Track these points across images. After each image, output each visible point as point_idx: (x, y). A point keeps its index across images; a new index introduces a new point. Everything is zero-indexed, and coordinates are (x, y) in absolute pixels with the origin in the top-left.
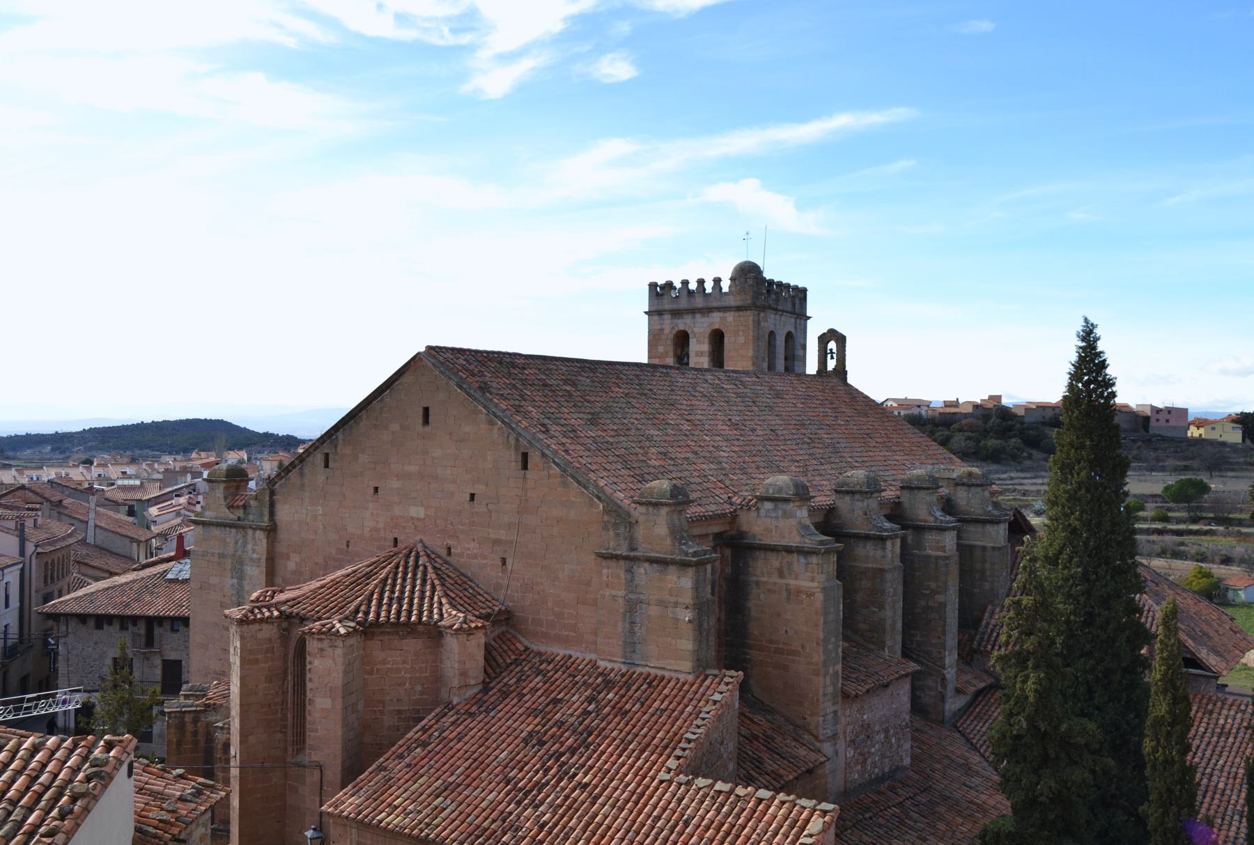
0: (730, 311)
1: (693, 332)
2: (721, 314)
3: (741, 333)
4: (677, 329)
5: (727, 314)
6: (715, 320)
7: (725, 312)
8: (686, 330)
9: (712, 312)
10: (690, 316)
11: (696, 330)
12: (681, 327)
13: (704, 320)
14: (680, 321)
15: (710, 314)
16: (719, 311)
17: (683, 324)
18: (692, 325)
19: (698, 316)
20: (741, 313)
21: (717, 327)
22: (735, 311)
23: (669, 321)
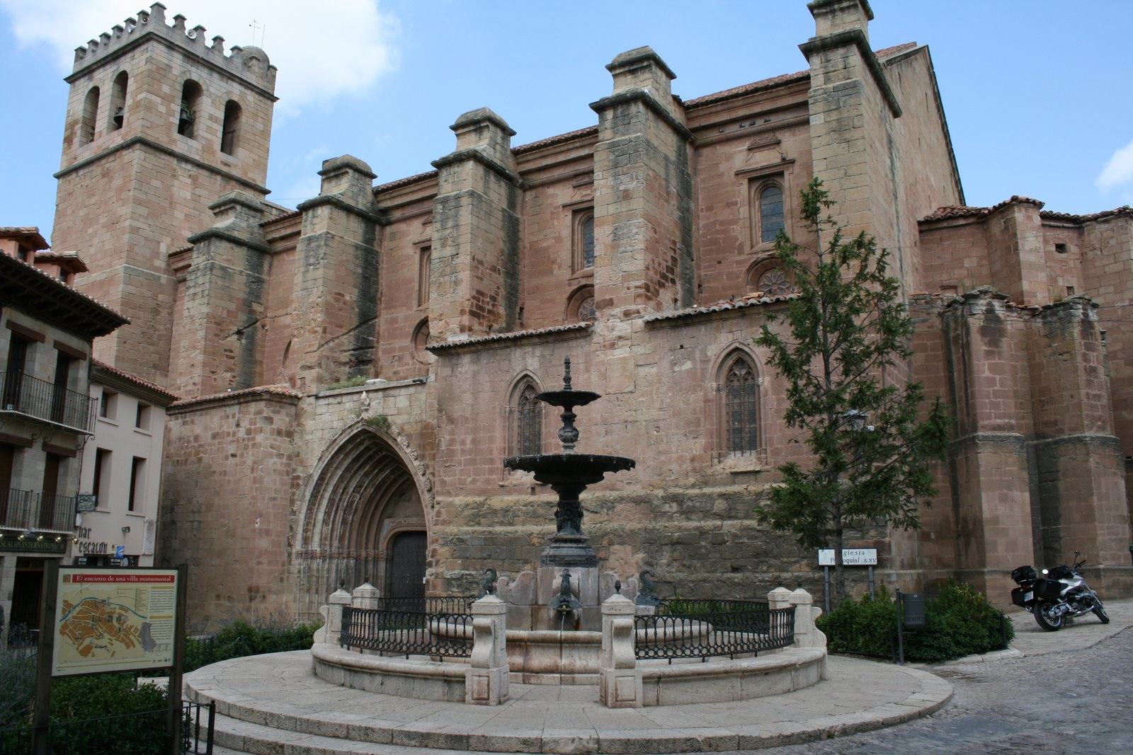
0: (252, 90)
1: (208, 90)
2: (242, 88)
3: (260, 119)
4: (188, 77)
5: (248, 92)
6: (236, 92)
7: (246, 87)
8: (201, 82)
9: (233, 80)
10: (206, 71)
11: (212, 90)
12: (195, 77)
13: (223, 84)
14: (193, 69)
15: (230, 82)
16: (241, 84)
17: (198, 74)
18: (208, 82)
19: (216, 76)
20: (261, 98)
21: (235, 99)
22: (257, 93)
23: (180, 62)
